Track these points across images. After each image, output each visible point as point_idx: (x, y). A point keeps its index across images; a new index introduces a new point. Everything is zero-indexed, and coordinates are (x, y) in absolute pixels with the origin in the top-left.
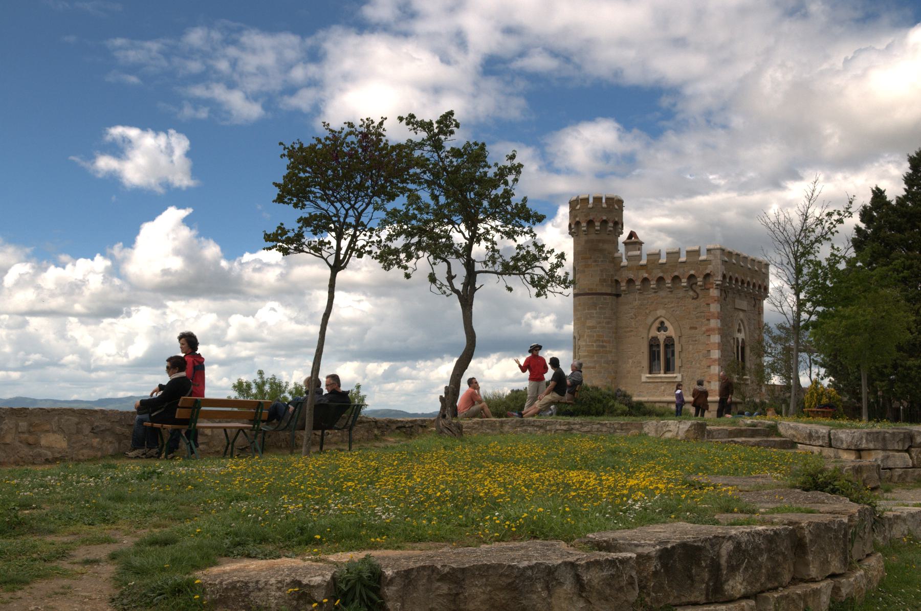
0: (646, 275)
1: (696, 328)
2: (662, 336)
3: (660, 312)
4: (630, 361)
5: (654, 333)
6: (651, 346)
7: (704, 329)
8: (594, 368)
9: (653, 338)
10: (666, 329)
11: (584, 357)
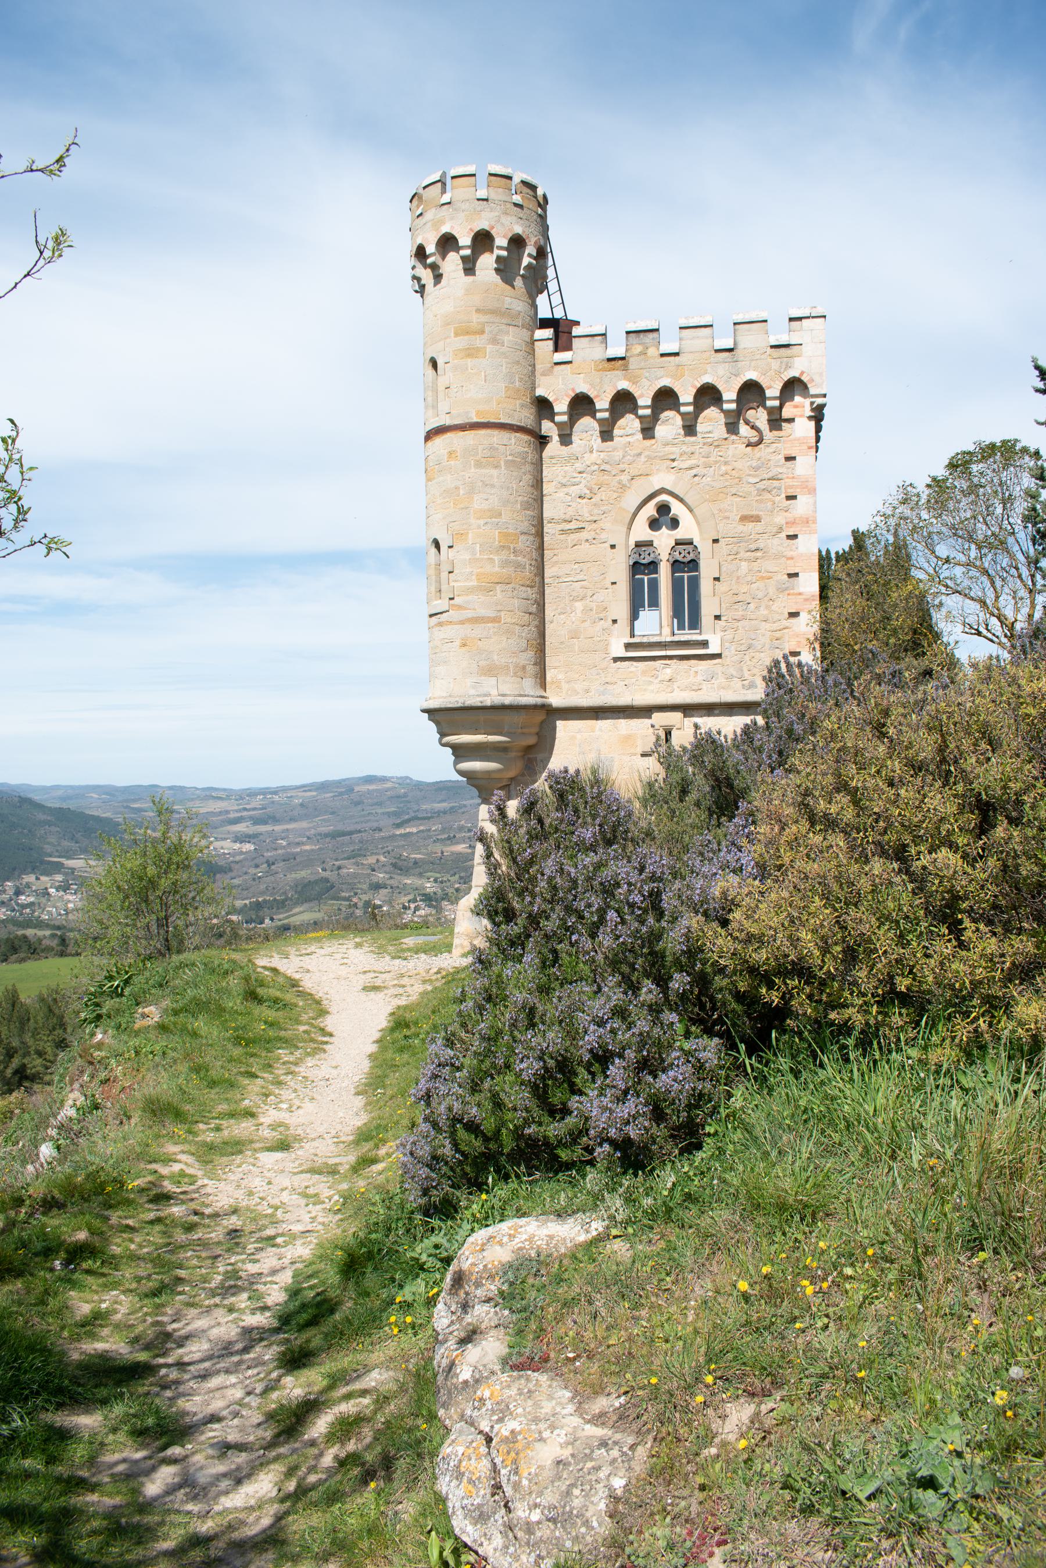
0: (623, 385)
1: (757, 519)
2: (664, 540)
3: (662, 479)
4: (579, 605)
5: (641, 531)
6: (636, 567)
7: (780, 519)
8: (496, 620)
9: (638, 545)
10: (675, 523)
11: (470, 590)
